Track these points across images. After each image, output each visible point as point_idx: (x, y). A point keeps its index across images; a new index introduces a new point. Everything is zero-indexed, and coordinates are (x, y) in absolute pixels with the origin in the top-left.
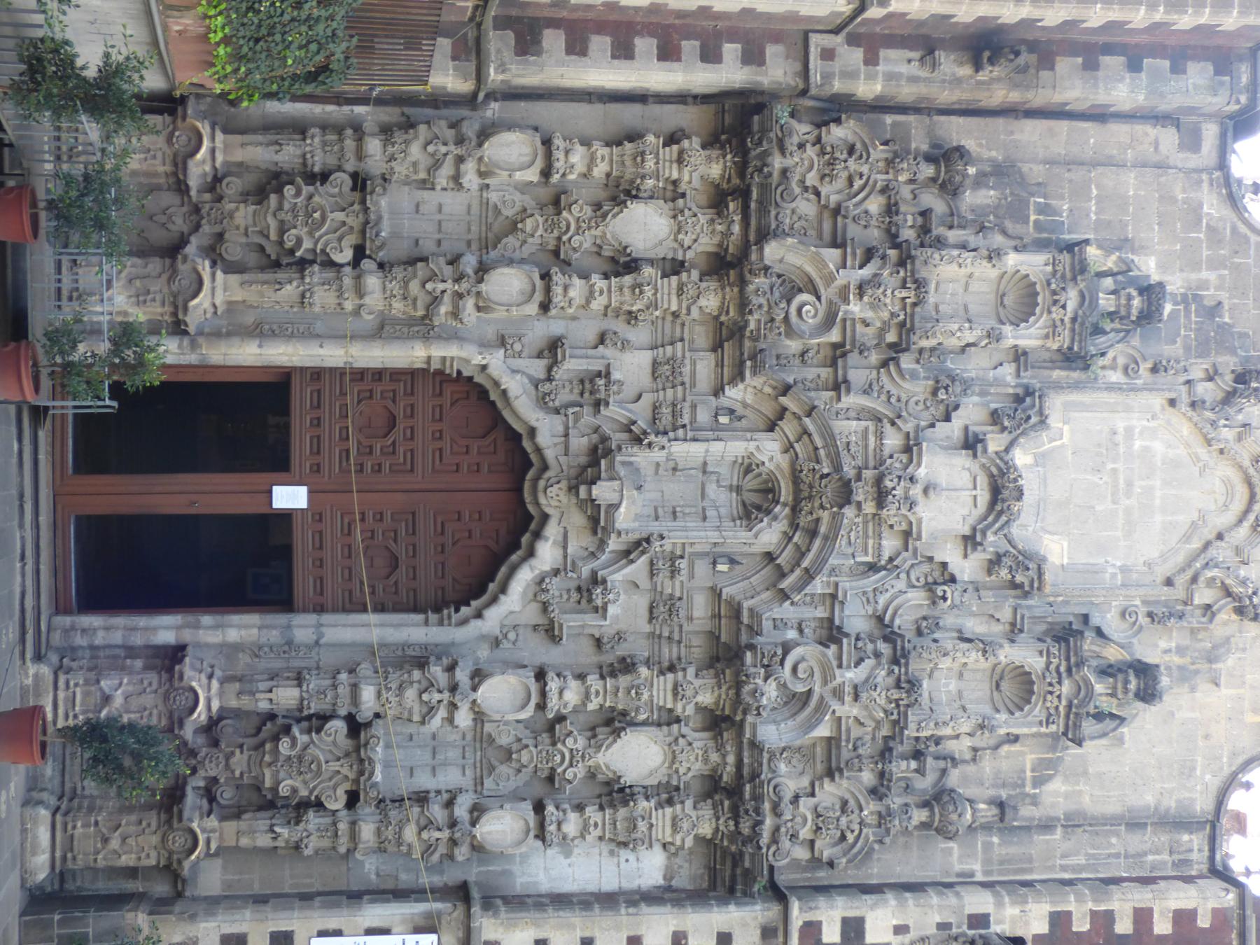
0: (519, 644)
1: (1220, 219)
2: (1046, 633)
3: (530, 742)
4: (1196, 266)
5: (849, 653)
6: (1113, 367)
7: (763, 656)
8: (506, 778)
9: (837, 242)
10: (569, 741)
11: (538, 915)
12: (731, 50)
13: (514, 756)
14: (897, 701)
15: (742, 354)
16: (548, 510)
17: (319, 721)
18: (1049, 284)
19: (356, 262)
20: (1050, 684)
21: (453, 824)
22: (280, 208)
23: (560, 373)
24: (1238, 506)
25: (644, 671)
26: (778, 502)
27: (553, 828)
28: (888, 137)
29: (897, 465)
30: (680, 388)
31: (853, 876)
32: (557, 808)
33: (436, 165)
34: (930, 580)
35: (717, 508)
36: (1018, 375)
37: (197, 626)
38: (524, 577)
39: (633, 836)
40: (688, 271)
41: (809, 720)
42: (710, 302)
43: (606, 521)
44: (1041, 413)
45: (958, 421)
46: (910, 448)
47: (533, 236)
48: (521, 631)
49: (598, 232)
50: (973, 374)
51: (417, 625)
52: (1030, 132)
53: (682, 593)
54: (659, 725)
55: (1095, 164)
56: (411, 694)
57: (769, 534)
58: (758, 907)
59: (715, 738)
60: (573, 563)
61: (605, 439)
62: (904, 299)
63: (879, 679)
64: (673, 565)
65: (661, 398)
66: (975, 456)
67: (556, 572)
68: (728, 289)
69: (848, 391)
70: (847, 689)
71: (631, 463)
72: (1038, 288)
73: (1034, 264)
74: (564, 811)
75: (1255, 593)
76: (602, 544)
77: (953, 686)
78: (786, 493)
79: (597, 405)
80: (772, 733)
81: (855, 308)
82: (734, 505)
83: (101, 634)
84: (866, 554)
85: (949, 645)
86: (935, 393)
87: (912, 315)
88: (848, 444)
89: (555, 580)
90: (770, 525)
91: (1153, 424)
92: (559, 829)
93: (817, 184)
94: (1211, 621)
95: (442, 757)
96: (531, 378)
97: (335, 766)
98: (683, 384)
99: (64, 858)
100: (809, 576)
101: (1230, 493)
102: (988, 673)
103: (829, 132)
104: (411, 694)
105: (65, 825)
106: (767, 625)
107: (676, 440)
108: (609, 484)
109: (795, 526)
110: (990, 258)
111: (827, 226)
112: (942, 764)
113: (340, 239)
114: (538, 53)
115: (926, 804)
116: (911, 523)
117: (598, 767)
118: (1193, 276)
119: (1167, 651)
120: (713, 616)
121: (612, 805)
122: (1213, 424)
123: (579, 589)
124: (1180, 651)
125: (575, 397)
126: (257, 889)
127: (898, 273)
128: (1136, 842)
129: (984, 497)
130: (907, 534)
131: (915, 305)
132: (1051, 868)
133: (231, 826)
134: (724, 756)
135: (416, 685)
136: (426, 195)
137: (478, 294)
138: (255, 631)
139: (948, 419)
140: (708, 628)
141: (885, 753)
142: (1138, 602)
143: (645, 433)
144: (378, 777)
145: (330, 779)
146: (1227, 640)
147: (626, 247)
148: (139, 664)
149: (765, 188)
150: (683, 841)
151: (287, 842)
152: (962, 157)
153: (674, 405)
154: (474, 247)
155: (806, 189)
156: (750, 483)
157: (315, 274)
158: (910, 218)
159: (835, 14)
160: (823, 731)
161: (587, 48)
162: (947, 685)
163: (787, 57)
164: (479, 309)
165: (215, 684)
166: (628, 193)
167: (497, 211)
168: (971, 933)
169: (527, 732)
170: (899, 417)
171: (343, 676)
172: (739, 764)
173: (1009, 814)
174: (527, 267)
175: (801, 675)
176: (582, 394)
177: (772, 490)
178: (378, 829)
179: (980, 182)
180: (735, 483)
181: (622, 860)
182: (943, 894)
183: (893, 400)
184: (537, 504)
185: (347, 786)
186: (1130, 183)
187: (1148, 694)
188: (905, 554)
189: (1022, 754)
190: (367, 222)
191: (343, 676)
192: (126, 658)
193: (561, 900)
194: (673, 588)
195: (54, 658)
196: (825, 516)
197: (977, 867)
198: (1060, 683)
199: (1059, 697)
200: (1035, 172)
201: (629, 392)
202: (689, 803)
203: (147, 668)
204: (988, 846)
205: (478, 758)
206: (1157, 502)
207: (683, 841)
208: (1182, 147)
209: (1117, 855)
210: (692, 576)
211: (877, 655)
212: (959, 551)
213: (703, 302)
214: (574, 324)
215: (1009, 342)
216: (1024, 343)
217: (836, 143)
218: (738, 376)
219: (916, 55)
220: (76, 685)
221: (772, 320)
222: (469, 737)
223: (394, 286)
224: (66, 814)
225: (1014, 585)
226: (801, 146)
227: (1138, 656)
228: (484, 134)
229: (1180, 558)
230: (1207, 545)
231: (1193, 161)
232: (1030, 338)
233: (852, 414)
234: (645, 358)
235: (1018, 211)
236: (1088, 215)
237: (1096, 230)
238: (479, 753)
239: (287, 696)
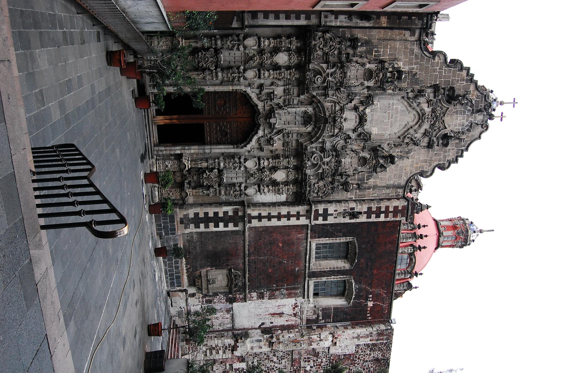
1: (418, 53)
2: (371, 149)
3: (257, 173)
4: (412, 64)
5: (326, 155)
6: (390, 89)
7: (307, 156)
8: (252, 180)
9: (327, 62)
10: (266, 173)
11: (258, 208)
12: (303, 16)
14: (336, 165)
15: (304, 88)
17: (211, 170)
18: (376, 72)
19: (215, 69)
20: (371, 161)
21: (241, 190)
22: (198, 57)
23: (263, 92)
24: (416, 120)
25: (282, 159)
27: (262, 191)
28: (340, 36)
29: (339, 114)
31: (326, 199)
32: (263, 186)
33: (234, 46)
34: (346, 138)
35: (298, 121)
36: (368, 92)
37: (185, 149)
38: (255, 138)
40: (292, 70)
42: (297, 76)
44: (372, 101)
45: (354, 103)
46: (342, 110)
48: (255, 149)
50: (358, 91)
51: (232, 148)
52: (374, 32)
54: (285, 169)
55: (390, 40)
56: (231, 164)
57: (309, 129)
58: (305, 207)
59: (297, 172)
60: (266, 134)
61: (273, 108)
62: (341, 76)
63: (333, 161)
64: (288, 135)
66: (356, 112)
67: (262, 137)
68: (301, 74)
69: (328, 97)
71: (279, 113)
72: (373, 72)
73: (372, 66)
74: (264, 187)
75: (418, 140)
76: (272, 131)
77: (350, 160)
79: (271, 100)
80: (308, 172)
81: (330, 79)
83: (164, 151)
85: (348, 152)
86: (348, 96)
87: (343, 80)
88: (328, 108)
90: (310, 126)
91: (399, 102)
92: (263, 191)
94: (408, 146)
97: (215, 179)
98: (291, 95)
99: (161, 197)
100: (318, 138)
102: (357, 158)
103: (326, 35)
104: (231, 164)
105: (161, 191)
106: (309, 148)
107: (289, 107)
108: (274, 119)
109: (315, 126)
111: (325, 57)
112: (346, 177)
113: (212, 64)
114: (257, 18)
115: (341, 185)
118: (411, 67)
119: (397, 152)
120: (297, 146)
122: (412, 102)
123: (267, 140)
124: (401, 152)
125: (266, 98)
126: (200, 202)
128: (388, 191)
129: (358, 121)
130: (340, 129)
131: (344, 78)
132: (369, 197)
133: (194, 191)
134: (299, 176)
136: (231, 51)
137: (244, 76)
138: (197, 150)
139: (351, 102)
141: (334, 175)
142: (392, 142)
143: (282, 106)
144: (225, 181)
145: (215, 182)
146: (412, 149)
147: (278, 63)
148: (173, 158)
149: (310, 50)
150: (290, 193)
151: (206, 194)
152: (357, 41)
154: (243, 63)
155: (320, 49)
157: (207, 72)
158: (344, 55)
160: (320, 171)
161: (268, 17)
162: (348, 160)
163: (316, 18)
164: (244, 79)
165: (189, 162)
166: (278, 50)
167: (248, 55)
168: (350, 211)
169: (256, 170)
170: (340, 102)
171: (217, 160)
173: (361, 186)
174: (255, 69)
176: (268, 97)
178: (225, 191)
179: (361, 46)
181: (277, 196)
182: (345, 203)
183: (339, 98)
184: (258, 122)
185: (218, 183)
186: (398, 44)
187: (393, 162)
188: (340, 133)
189: (364, 174)
190: (218, 61)
191: (217, 160)
192: (170, 156)
193: (264, 205)
195: (155, 157)
197: (353, 197)
198: (373, 161)
199: (372, 164)
200: (375, 41)
201: (278, 97)
202: (291, 185)
203: (175, 159)
204: (356, 193)
206: (398, 119)
207: (290, 193)
208: (411, 36)
209: (384, 194)
210: (292, 137)
211: (333, 155)
212: (352, 132)
213: (296, 76)
214: (266, 81)
215: (366, 85)
216: (369, 85)
217: (328, 37)
218: (303, 94)
219: (346, 16)
220: (160, 163)
221: (311, 81)
222: (244, 171)
223: (225, 75)
224: (161, 189)
225: (364, 139)
226: (319, 38)
227: (391, 153)
228: (245, 37)
229: (403, 132)
230: (409, 129)
231: (413, 39)
232: (371, 84)
233: (329, 102)
234: (282, 88)
235: (370, 52)
237: (389, 56)
239: (205, 165)
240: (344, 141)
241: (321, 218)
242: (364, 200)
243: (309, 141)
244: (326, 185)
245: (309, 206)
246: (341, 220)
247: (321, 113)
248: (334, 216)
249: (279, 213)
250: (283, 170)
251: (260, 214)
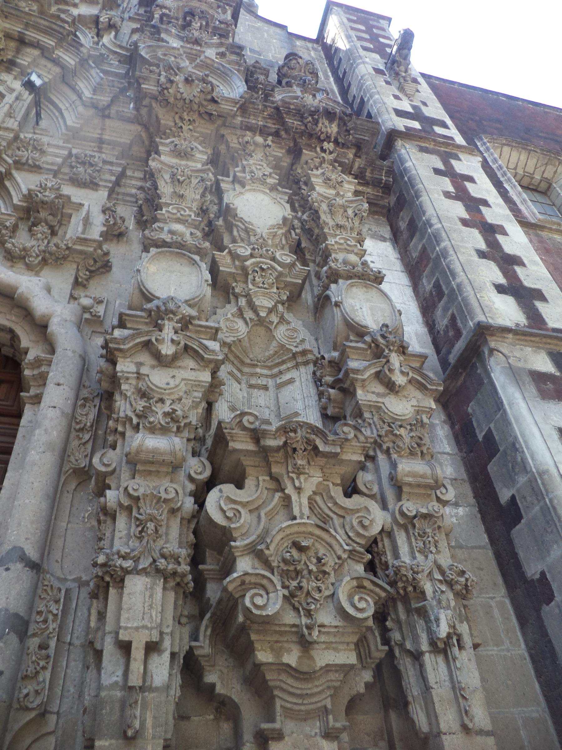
53: (63, 148)
95: (267, 411)
132: (329, 83)
135: (144, 370)
205: (265, 372)
238: (258, 370)
245: (399, 143)
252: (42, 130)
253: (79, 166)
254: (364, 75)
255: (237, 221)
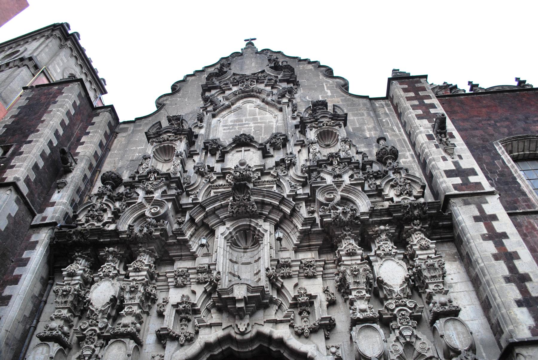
0: (337, 344)
3: (397, 332)
13: (408, 340)
16: (254, 332)
24: (254, 99)
26: (250, 225)
30: (189, 271)
36: (198, 154)
39: (436, 265)
41: (355, 194)
43: (256, 292)
47: (94, 351)
49: (100, 316)
54: (372, 267)
65: (194, 280)
67: (292, 326)
70: (336, 180)
76: (272, 301)
78: (244, 222)
79: (196, 312)
81: (157, 195)
82: (253, 249)
84: (272, 187)
87: (162, 174)
89: (296, 325)
93: (102, 223)
96: (177, 350)
98: (187, 271)
101: (249, 102)
109: (260, 216)
110: (146, 159)
116: (257, 170)
117: (403, 290)
121: (423, 282)
127: (144, 182)
131: (158, 174)
132: (401, 135)
134: (382, 231)
140: (317, 252)
153: (198, 272)
156: (242, 244)
159: (17, 201)
172: (384, 223)
175: (332, 196)
177: (245, 231)
180: (243, 250)
181: (452, 281)
194: (296, 266)
196: (253, 198)
207: (432, 243)
230: (267, 103)
234: (172, 291)
236: (142, 149)
240: (290, 170)
241: (472, 179)
242: (409, 135)
243: (292, 222)
244: (391, 183)
245: (452, 200)
246: (459, 141)
247: (227, 205)
248: (457, 159)
249: (496, 257)
250: (376, 268)
251: (519, 304)
252: (284, 248)
253: (307, 268)
254: (422, 144)
255: (384, 285)
